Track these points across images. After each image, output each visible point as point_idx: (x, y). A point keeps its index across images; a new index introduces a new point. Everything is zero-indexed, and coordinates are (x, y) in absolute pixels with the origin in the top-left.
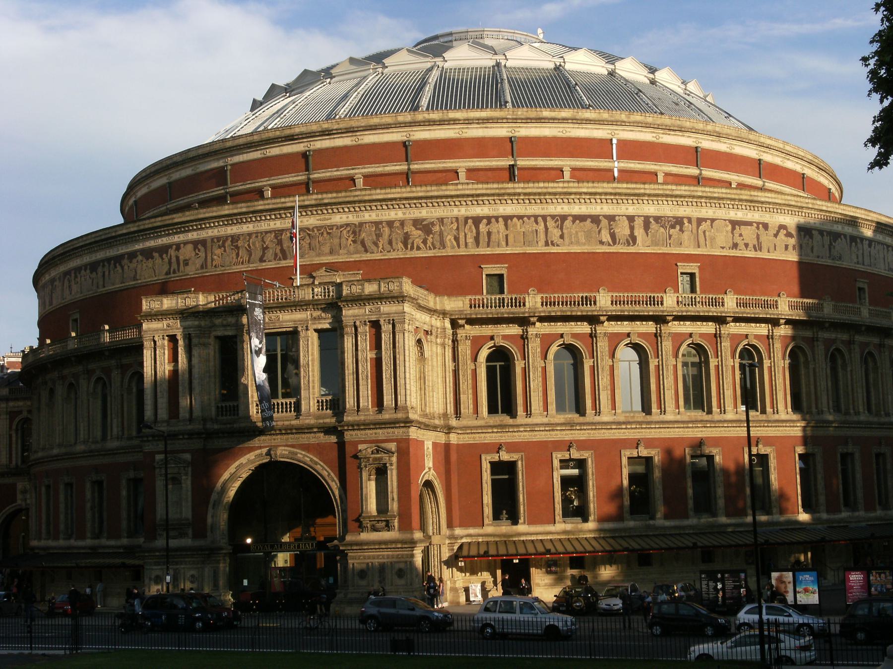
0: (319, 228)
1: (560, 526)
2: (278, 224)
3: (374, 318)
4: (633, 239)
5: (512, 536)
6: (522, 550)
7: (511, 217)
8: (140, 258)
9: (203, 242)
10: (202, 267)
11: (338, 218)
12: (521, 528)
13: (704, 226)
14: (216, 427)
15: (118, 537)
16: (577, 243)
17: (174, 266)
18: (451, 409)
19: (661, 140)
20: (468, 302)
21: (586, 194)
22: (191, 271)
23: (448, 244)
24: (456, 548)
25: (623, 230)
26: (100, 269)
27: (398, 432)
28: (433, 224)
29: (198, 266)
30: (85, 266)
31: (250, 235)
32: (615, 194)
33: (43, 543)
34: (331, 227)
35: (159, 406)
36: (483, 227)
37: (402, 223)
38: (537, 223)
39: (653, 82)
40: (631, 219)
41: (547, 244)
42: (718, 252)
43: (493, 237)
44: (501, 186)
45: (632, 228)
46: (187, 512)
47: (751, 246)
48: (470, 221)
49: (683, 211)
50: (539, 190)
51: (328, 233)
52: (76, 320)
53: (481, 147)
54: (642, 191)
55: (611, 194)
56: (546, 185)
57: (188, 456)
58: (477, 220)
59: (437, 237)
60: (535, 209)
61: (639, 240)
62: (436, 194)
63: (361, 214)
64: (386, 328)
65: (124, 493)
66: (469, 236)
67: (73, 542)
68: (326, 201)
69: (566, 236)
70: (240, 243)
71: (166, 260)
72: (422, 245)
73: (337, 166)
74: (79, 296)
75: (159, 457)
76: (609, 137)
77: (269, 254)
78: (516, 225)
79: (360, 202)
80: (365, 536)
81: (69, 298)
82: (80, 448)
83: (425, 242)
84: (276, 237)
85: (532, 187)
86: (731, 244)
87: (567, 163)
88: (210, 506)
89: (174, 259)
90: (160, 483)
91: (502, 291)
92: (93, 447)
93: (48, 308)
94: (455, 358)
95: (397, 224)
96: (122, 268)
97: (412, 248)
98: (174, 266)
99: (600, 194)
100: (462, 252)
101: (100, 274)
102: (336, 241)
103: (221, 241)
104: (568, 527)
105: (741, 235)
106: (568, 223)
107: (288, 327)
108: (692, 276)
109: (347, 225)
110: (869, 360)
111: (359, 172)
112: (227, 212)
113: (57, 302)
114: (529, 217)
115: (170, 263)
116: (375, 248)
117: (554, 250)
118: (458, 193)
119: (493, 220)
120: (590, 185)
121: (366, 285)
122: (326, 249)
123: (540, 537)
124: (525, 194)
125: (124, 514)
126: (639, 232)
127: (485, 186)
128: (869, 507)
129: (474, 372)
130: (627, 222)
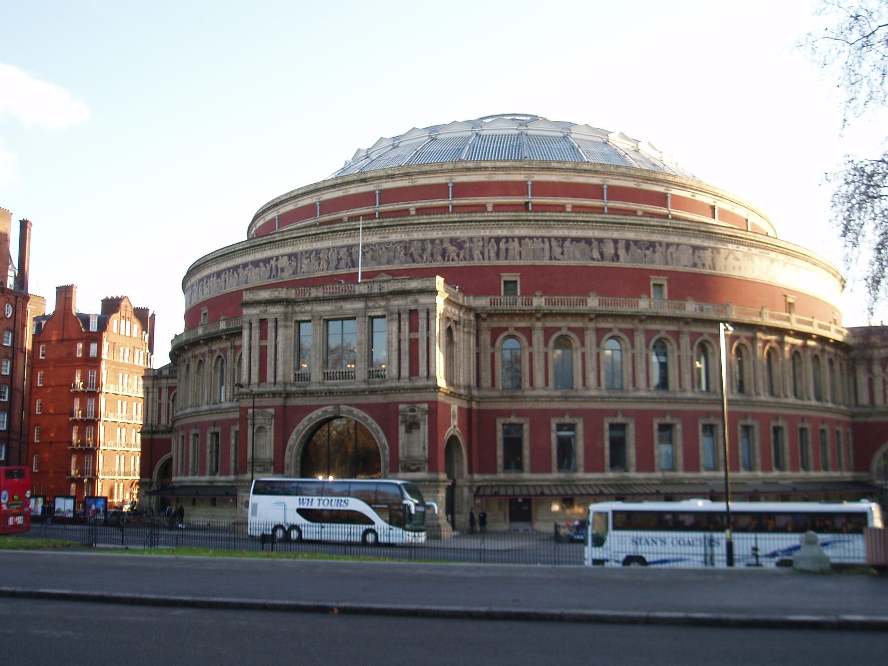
0: (379, 244)
1: (556, 475)
2: (350, 241)
3: (413, 307)
4: (616, 257)
5: (519, 481)
6: (525, 492)
7: (524, 238)
8: (250, 267)
9: (295, 255)
10: (294, 273)
11: (394, 237)
12: (526, 475)
13: (672, 249)
14: (294, 389)
16: (573, 258)
17: (274, 272)
18: (473, 382)
19: (641, 187)
20: (488, 300)
21: (581, 221)
22: (287, 276)
23: (476, 257)
24: (474, 489)
25: (609, 249)
26: (223, 276)
27: (428, 396)
28: (464, 242)
29: (291, 272)
30: (213, 274)
31: (329, 249)
32: (603, 222)
33: (179, 478)
34: (388, 243)
35: (252, 372)
36: (502, 245)
37: (442, 241)
38: (543, 242)
39: (637, 151)
40: (615, 241)
41: (551, 259)
42: (681, 269)
43: (510, 252)
44: (517, 214)
45: (616, 249)
47: (707, 266)
48: (493, 240)
49: (655, 238)
50: (546, 218)
51: (386, 248)
53: (505, 188)
54: (624, 221)
55: (600, 222)
56: (551, 214)
57: (272, 411)
58: (498, 240)
59: (467, 251)
61: (622, 258)
62: (467, 219)
63: (411, 234)
65: (233, 442)
66: (491, 251)
67: (197, 478)
68: (385, 224)
69: (565, 253)
70: (321, 255)
71: (269, 268)
72: (456, 258)
73: (397, 201)
74: (209, 297)
75: (250, 411)
76: (601, 183)
77: (343, 263)
78: (527, 244)
79: (410, 224)
81: (202, 298)
82: (205, 407)
83: (458, 255)
84: (348, 251)
85: (540, 216)
86: (691, 264)
87: (569, 202)
88: (287, 450)
89: (274, 267)
90: (250, 431)
91: (516, 294)
92: (213, 407)
94: (478, 344)
95: (437, 242)
96: (238, 274)
97: (448, 260)
98: (274, 272)
99: (592, 222)
100: (486, 263)
101: (223, 279)
102: (392, 254)
103: (308, 254)
104: (562, 475)
105: (699, 257)
106: (567, 243)
108: (661, 286)
109: (401, 242)
110: (796, 357)
111: (412, 206)
112: (313, 232)
113: (195, 301)
114: (538, 238)
115: (271, 271)
116: (419, 258)
117: (556, 263)
118: (485, 219)
119: (510, 240)
120: (585, 215)
121: (408, 282)
122: (384, 259)
123: (540, 483)
124: (535, 221)
125: (232, 457)
126: (622, 252)
127: (505, 214)
128: (794, 469)
129: (493, 355)
130: (612, 244)
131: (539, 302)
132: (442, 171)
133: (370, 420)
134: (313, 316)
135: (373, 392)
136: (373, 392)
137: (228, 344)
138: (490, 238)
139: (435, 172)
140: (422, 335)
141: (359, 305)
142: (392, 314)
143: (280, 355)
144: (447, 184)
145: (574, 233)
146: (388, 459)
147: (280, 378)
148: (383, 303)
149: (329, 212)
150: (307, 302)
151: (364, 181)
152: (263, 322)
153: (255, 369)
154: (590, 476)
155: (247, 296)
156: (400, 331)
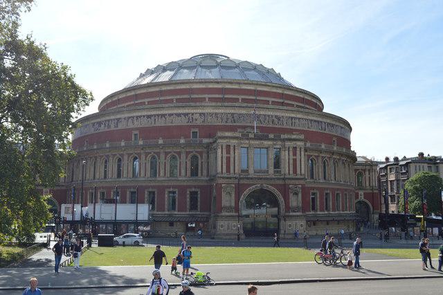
1: (312, 212)
2: (233, 111)
4: (325, 130)
9: (204, 114)
15: (164, 211)
22: (199, 122)
27: (302, 182)
30: (144, 116)
37: (272, 116)
46: (233, 204)
49: (334, 123)
52: (135, 135)
57: (234, 185)
58: (292, 118)
64: (298, 149)
65: (166, 196)
80: (291, 214)
81: (131, 126)
93: (113, 128)
100: (288, 127)
103: (211, 114)
111: (241, 97)
131: (308, 145)
132: (254, 84)
135: (278, 179)
136: (278, 179)
137: (162, 151)
139: (250, 84)
141: (270, 143)
143: (236, 161)
144: (255, 90)
146: (284, 207)
147: (236, 171)
149: (198, 94)
150: (247, 139)
151: (218, 83)
152: (228, 147)
153: (224, 167)
154: (321, 213)
155: (219, 134)
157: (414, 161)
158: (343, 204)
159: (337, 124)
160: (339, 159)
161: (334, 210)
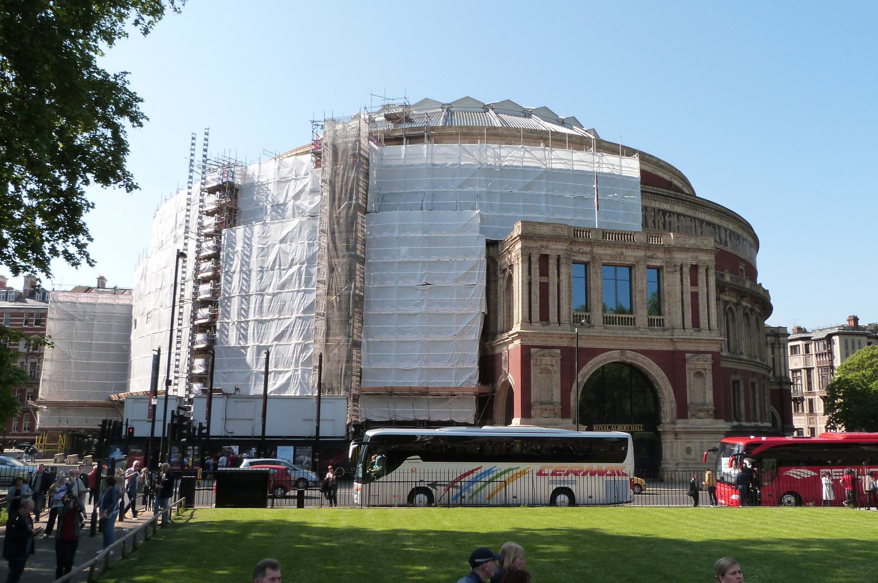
4: (726, 244)
36: (667, 217)
40: (726, 229)
46: (557, 397)
57: (559, 351)
58: (664, 212)
60: (690, 213)
107: (630, 261)
126: (728, 239)
133: (656, 367)
134: (593, 258)
138: (659, 210)
140: (702, 289)
141: (641, 253)
142: (675, 266)
145: (708, 218)
148: (660, 255)
152: (544, 259)
156: (682, 284)
157: (843, 333)
158: (760, 407)
159: (745, 235)
160: (752, 310)
161: (748, 420)
